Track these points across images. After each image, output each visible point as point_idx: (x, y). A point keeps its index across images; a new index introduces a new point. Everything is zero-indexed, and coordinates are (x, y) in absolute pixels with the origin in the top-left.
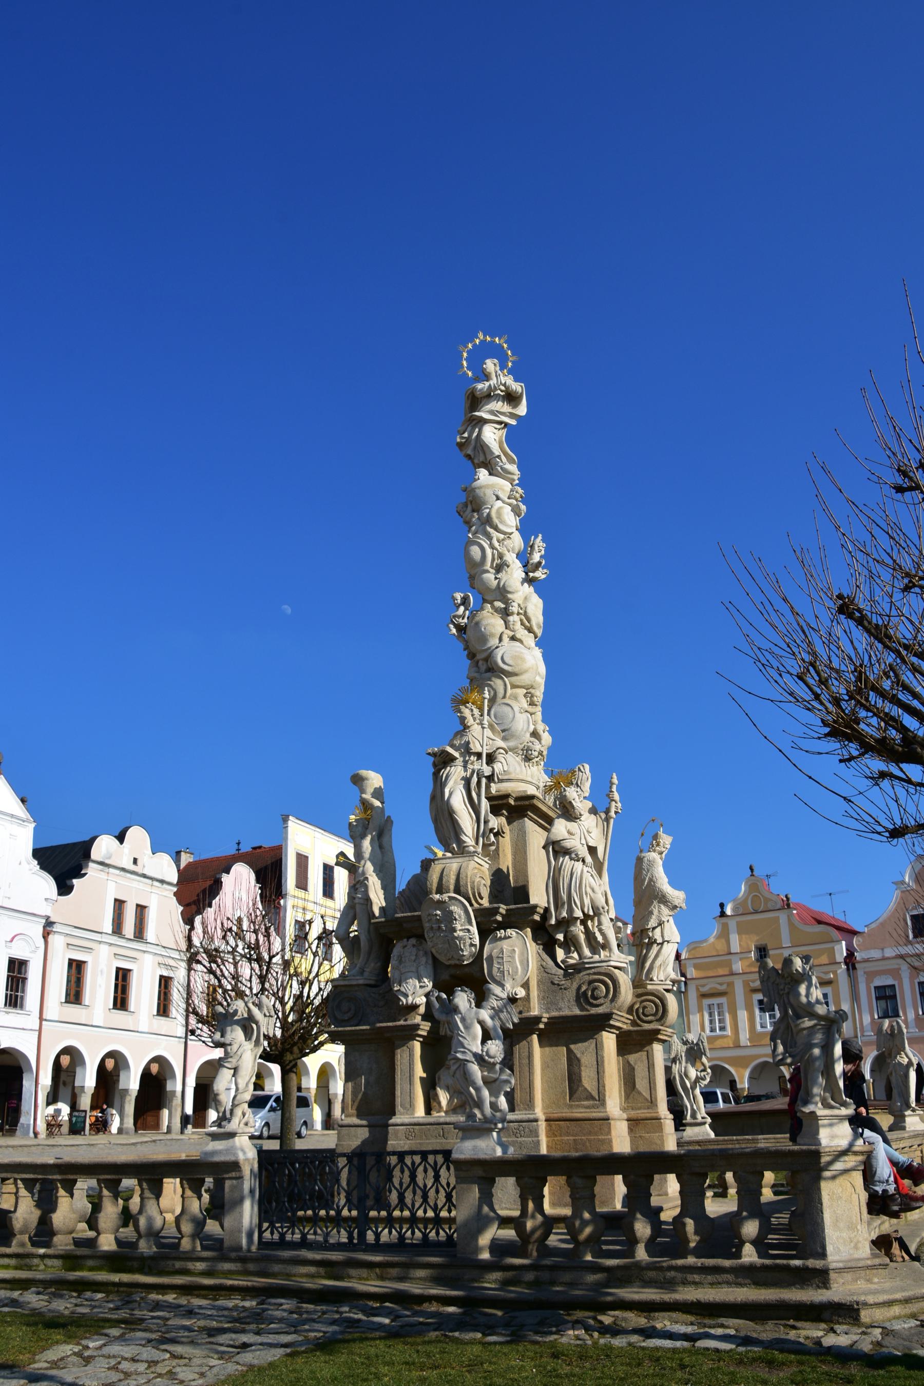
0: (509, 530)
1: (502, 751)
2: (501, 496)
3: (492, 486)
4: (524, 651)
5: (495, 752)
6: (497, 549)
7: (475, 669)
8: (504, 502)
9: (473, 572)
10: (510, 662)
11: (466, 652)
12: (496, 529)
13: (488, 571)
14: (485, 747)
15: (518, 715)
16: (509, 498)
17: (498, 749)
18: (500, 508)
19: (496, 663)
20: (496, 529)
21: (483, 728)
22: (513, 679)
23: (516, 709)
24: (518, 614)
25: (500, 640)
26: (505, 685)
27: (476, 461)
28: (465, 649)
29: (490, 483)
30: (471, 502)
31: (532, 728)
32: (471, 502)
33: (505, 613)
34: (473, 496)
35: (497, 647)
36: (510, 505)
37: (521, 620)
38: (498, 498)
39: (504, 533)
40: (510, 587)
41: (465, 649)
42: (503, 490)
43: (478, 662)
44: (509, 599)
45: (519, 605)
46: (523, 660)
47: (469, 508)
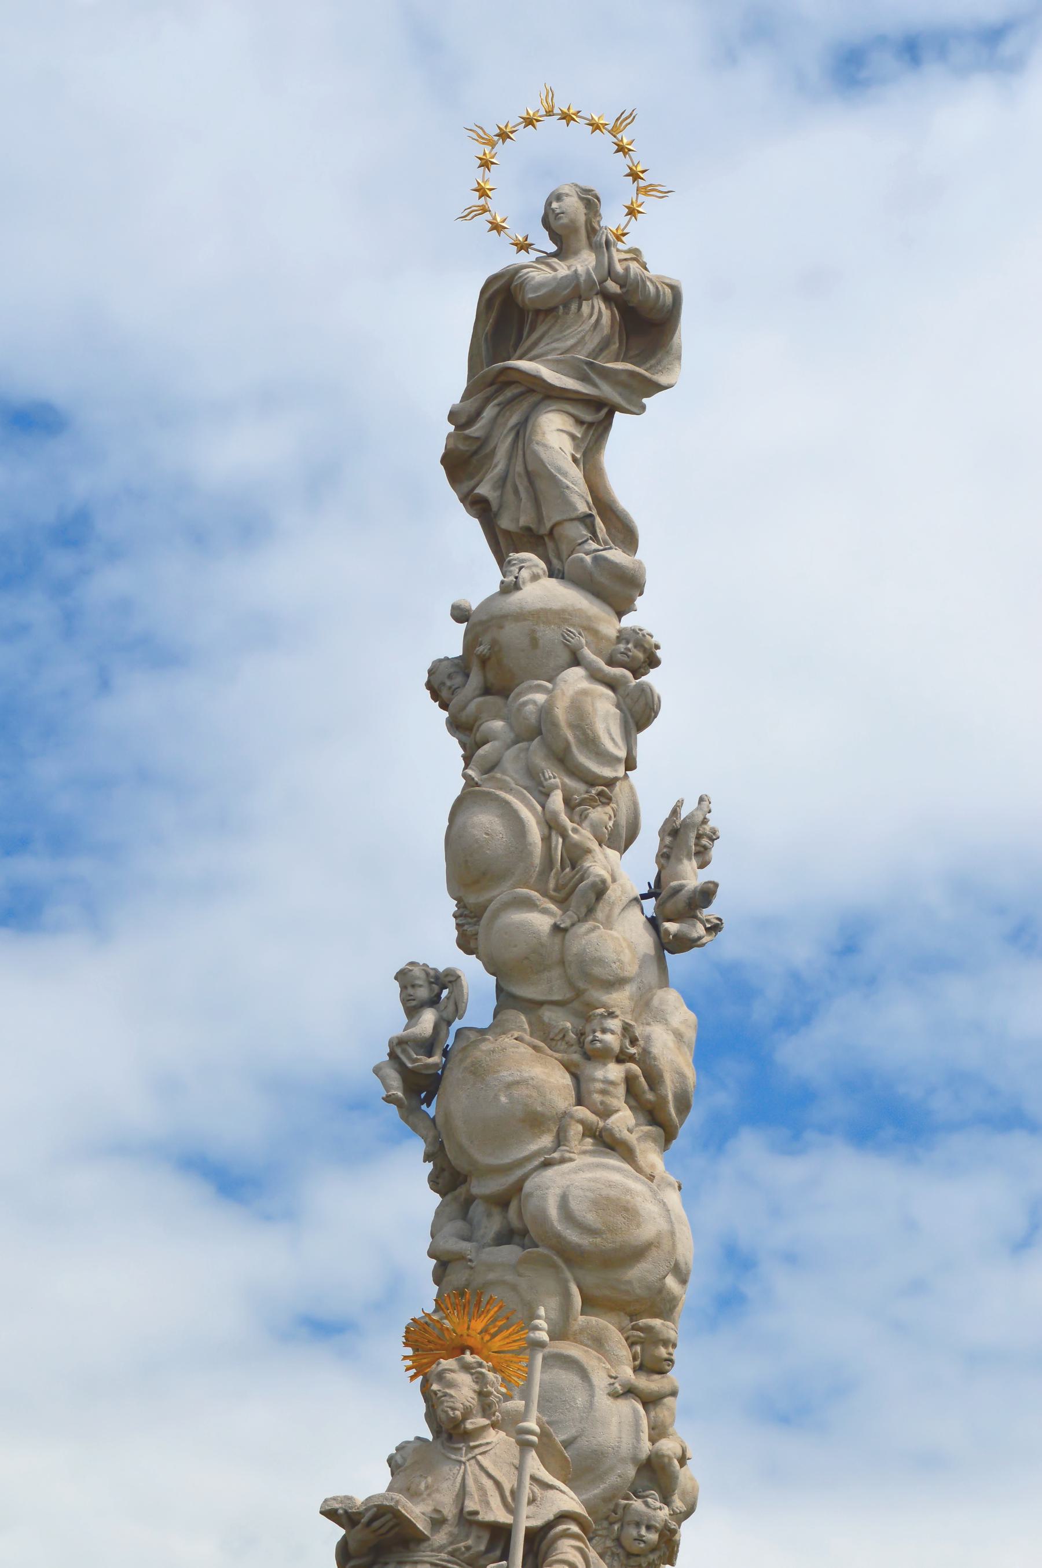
0: (607, 772)
1: (575, 1528)
2: (587, 653)
3: (561, 616)
4: (637, 1185)
5: (550, 1525)
6: (564, 835)
7: (459, 1225)
8: (596, 676)
9: (471, 899)
10: (591, 1218)
11: (429, 1166)
12: (563, 760)
13: (528, 904)
14: (525, 1510)
15: (603, 1400)
16: (611, 663)
17: (564, 1516)
18: (585, 692)
19: (542, 1218)
20: (563, 760)
21: (524, 1445)
22: (591, 1279)
23: (600, 1380)
24: (621, 1058)
25: (560, 1140)
26: (567, 1295)
27: (505, 523)
28: (427, 1158)
29: (556, 605)
30: (484, 661)
31: (646, 1447)
32: (484, 661)
33: (583, 1054)
34: (494, 643)
35: (547, 1164)
36: (612, 684)
37: (630, 1081)
38: (576, 660)
39: (591, 780)
40: (600, 961)
41: (427, 1158)
42: (592, 631)
43: (469, 1201)
44: (591, 1006)
45: (627, 1028)
46: (630, 1212)
47: (475, 680)
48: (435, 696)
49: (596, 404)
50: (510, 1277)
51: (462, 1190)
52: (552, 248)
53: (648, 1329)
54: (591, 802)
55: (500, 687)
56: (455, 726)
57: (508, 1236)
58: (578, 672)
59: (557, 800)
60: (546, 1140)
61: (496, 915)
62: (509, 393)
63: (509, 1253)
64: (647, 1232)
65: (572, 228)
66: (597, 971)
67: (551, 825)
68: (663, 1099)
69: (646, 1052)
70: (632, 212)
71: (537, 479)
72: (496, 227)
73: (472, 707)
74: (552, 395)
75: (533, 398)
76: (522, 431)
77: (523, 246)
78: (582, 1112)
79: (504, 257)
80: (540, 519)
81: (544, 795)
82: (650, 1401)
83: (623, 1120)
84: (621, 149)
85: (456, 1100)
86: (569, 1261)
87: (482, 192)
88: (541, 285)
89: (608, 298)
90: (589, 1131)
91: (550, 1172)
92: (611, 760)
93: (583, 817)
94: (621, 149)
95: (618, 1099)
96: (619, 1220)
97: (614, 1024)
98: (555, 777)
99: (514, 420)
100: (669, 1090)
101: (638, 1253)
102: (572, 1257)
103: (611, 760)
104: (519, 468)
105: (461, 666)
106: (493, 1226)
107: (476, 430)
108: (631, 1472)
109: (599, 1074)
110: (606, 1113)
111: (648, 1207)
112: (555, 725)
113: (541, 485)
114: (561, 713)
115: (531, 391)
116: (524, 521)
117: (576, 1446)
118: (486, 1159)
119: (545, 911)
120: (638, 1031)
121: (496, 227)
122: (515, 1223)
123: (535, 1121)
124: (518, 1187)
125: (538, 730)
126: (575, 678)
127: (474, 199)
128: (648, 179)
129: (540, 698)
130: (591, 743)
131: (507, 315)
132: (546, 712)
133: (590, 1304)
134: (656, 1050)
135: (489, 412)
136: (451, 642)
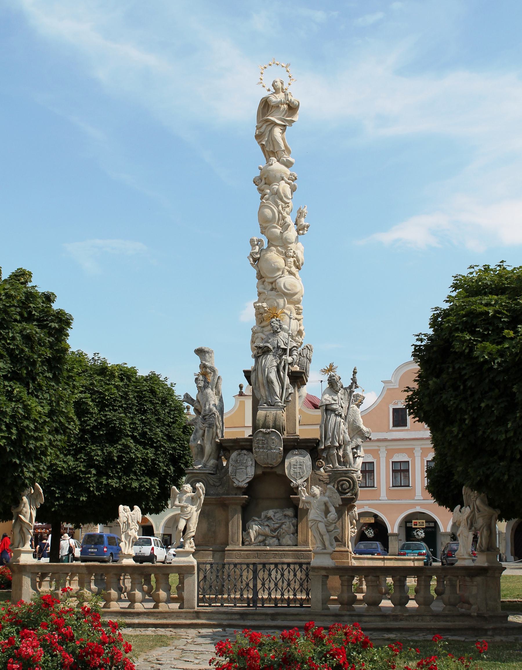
6: (282, 214)
8: (286, 183)
9: (264, 225)
12: (281, 199)
19: (280, 288)
20: (281, 199)
25: (283, 273)
33: (286, 256)
35: (281, 277)
37: (294, 261)
38: (283, 179)
43: (264, 281)
45: (294, 252)
48: (254, 183)
49: (285, 126)
50: (274, 298)
51: (263, 279)
52: (274, 91)
53: (298, 307)
55: (269, 183)
57: (272, 289)
58: (283, 181)
59: (280, 207)
60: (281, 273)
61: (269, 229)
62: (269, 123)
64: (297, 290)
65: (279, 89)
66: (288, 241)
67: (279, 212)
69: (297, 256)
71: (273, 141)
75: (273, 125)
76: (271, 131)
77: (269, 90)
78: (287, 268)
80: (274, 149)
82: (299, 320)
83: (294, 269)
85: (262, 263)
86: (285, 295)
89: (286, 104)
90: (288, 271)
93: (284, 210)
95: (292, 265)
97: (292, 251)
98: (280, 202)
99: (270, 129)
100: (301, 263)
101: (296, 294)
102: (285, 294)
104: (270, 139)
106: (270, 287)
107: (262, 130)
108: (296, 333)
109: (289, 260)
110: (290, 267)
112: (280, 193)
113: (275, 143)
114: (281, 191)
115: (272, 123)
118: (269, 275)
120: (296, 252)
122: (274, 287)
123: (278, 269)
124: (275, 281)
126: (283, 182)
129: (277, 187)
130: (286, 197)
131: (266, 106)
132: (278, 190)
133: (289, 303)
134: (299, 256)
135: (264, 127)
136: (258, 173)
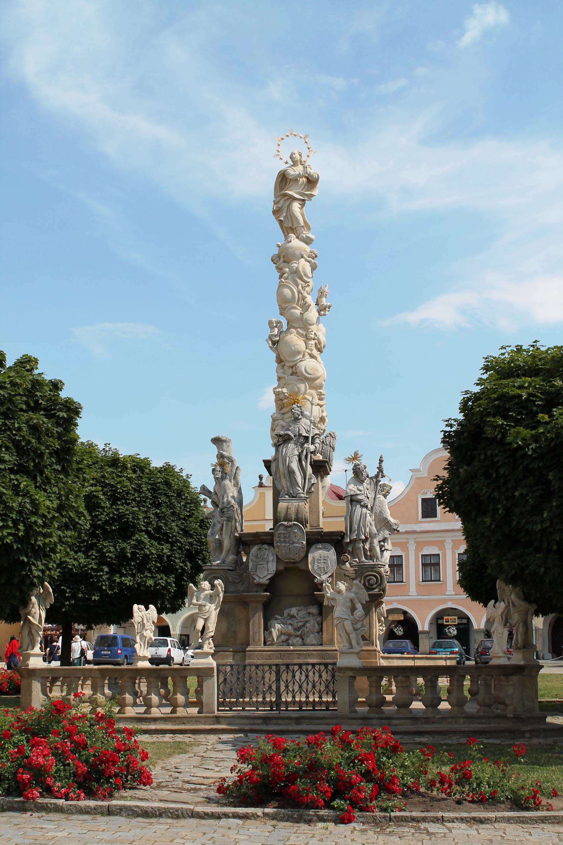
2: (305, 256)
6: (302, 294)
8: (306, 260)
9: (283, 306)
12: (301, 279)
19: (301, 372)
20: (301, 279)
25: (304, 356)
26: (306, 386)
33: (307, 338)
35: (301, 361)
37: (316, 344)
38: (302, 257)
40: (310, 320)
43: (284, 366)
45: (315, 334)
48: (272, 261)
49: (304, 200)
50: (295, 382)
51: (283, 363)
52: (292, 164)
53: (320, 392)
54: (306, 287)
55: (287, 262)
56: (277, 268)
57: (292, 374)
58: (303, 260)
59: (300, 286)
60: (301, 356)
61: (289, 310)
62: (286, 198)
63: (294, 377)
64: (320, 374)
65: (297, 161)
66: (309, 322)
67: (299, 292)
68: (321, 347)
69: (318, 338)
70: (308, 156)
71: (291, 216)
72: (281, 159)
73: (281, 266)
74: (295, 199)
75: (291, 200)
76: (289, 206)
77: (287, 163)
78: (308, 350)
79: (283, 167)
80: (293, 225)
81: (297, 286)
82: (321, 406)
83: (315, 352)
84: (306, 142)
85: (281, 346)
86: (306, 379)
87: (278, 151)
88: (292, 175)
89: (305, 177)
90: (309, 354)
91: (302, 362)
92: (309, 277)
93: (305, 289)
94: (306, 142)
95: (314, 348)
96: (315, 372)
97: (313, 333)
98: (299, 281)
99: (288, 204)
100: (322, 345)
101: (317, 378)
102: (307, 379)
103: (309, 277)
104: (289, 214)
105: (279, 256)
106: (290, 371)
107: (280, 205)
108: (319, 419)
109: (310, 342)
110: (311, 350)
111: (320, 369)
112: (299, 272)
113: (293, 219)
114: (301, 269)
115: (290, 198)
116: (289, 226)
117: (353, 675)
118: (288, 359)
119: (299, 310)
120: (317, 334)
121: (281, 159)
122: (294, 371)
123: (299, 353)
124: (296, 365)
125: (296, 272)
126: (302, 260)
127: (277, 153)
128: (311, 149)
129: (296, 265)
130: (306, 275)
131: (283, 179)
132: (297, 268)
133: (310, 388)
134: (320, 338)
135: (282, 201)
136: (276, 251)
